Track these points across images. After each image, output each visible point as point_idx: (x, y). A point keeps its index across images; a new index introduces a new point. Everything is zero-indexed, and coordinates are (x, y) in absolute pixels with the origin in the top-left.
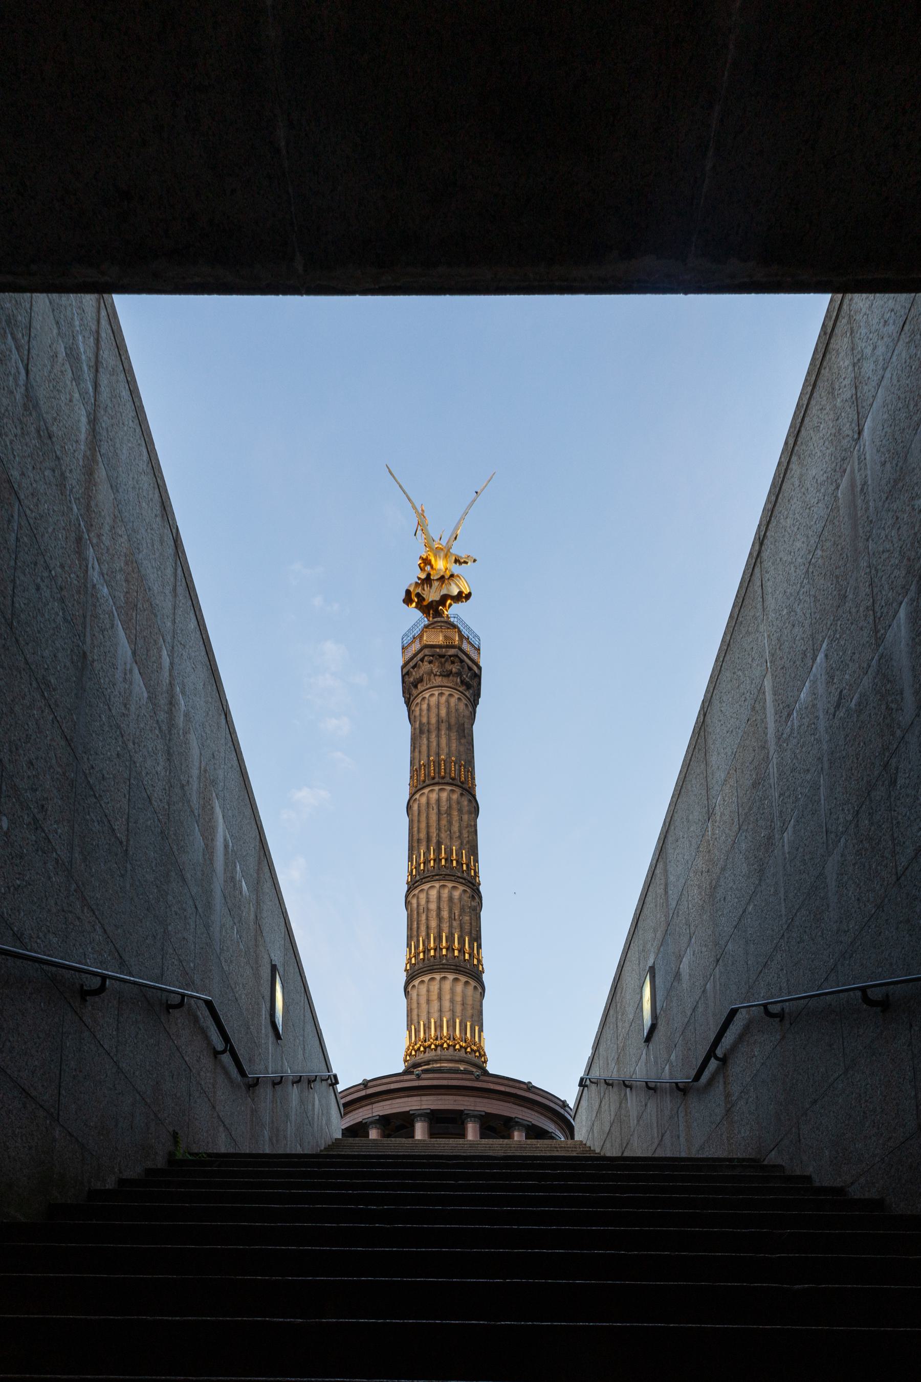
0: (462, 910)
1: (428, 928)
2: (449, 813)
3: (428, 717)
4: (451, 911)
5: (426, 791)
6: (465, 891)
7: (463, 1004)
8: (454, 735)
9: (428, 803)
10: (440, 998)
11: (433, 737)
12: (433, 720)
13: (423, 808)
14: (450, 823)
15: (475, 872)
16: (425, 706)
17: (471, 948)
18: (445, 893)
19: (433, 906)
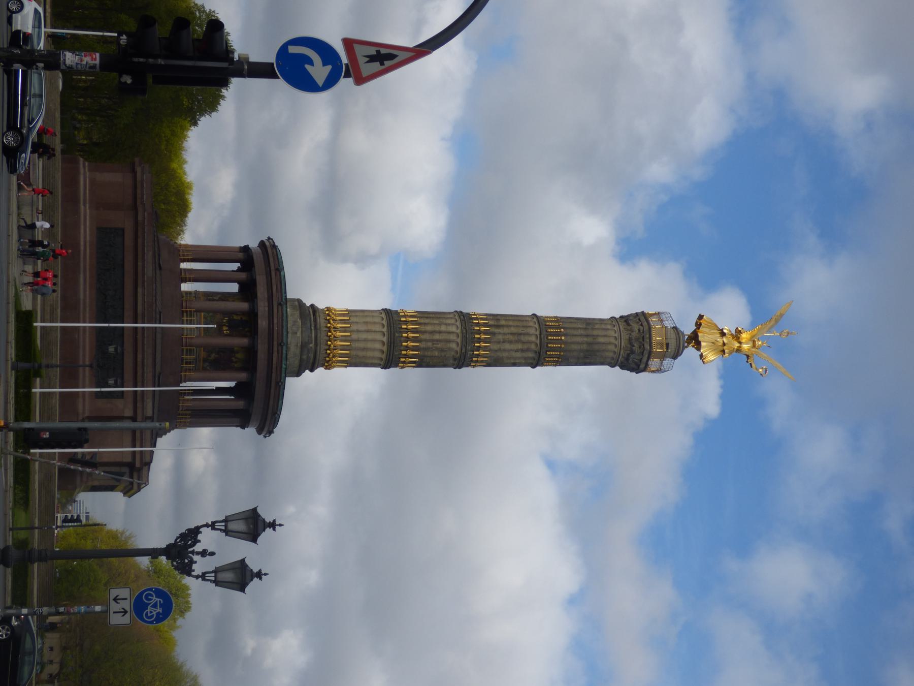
0: (442, 350)
1: (425, 324)
2: (517, 342)
3: (598, 329)
4: (438, 341)
5: (537, 326)
6: (457, 352)
7: (364, 349)
8: (585, 347)
9: (527, 327)
10: (368, 331)
11: (582, 332)
12: (595, 333)
13: (525, 324)
14: (511, 342)
15: (476, 362)
16: (609, 327)
17: (413, 356)
18: (453, 337)
19: (443, 328)
